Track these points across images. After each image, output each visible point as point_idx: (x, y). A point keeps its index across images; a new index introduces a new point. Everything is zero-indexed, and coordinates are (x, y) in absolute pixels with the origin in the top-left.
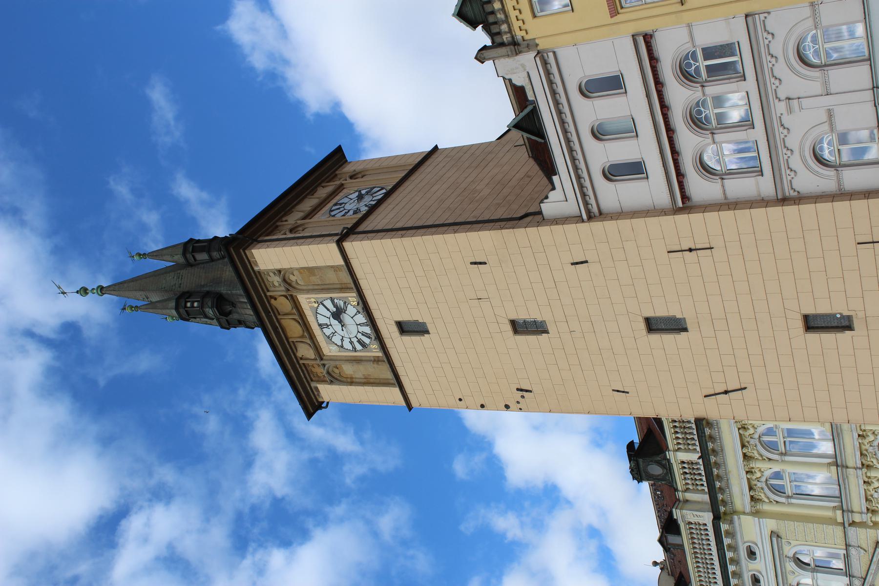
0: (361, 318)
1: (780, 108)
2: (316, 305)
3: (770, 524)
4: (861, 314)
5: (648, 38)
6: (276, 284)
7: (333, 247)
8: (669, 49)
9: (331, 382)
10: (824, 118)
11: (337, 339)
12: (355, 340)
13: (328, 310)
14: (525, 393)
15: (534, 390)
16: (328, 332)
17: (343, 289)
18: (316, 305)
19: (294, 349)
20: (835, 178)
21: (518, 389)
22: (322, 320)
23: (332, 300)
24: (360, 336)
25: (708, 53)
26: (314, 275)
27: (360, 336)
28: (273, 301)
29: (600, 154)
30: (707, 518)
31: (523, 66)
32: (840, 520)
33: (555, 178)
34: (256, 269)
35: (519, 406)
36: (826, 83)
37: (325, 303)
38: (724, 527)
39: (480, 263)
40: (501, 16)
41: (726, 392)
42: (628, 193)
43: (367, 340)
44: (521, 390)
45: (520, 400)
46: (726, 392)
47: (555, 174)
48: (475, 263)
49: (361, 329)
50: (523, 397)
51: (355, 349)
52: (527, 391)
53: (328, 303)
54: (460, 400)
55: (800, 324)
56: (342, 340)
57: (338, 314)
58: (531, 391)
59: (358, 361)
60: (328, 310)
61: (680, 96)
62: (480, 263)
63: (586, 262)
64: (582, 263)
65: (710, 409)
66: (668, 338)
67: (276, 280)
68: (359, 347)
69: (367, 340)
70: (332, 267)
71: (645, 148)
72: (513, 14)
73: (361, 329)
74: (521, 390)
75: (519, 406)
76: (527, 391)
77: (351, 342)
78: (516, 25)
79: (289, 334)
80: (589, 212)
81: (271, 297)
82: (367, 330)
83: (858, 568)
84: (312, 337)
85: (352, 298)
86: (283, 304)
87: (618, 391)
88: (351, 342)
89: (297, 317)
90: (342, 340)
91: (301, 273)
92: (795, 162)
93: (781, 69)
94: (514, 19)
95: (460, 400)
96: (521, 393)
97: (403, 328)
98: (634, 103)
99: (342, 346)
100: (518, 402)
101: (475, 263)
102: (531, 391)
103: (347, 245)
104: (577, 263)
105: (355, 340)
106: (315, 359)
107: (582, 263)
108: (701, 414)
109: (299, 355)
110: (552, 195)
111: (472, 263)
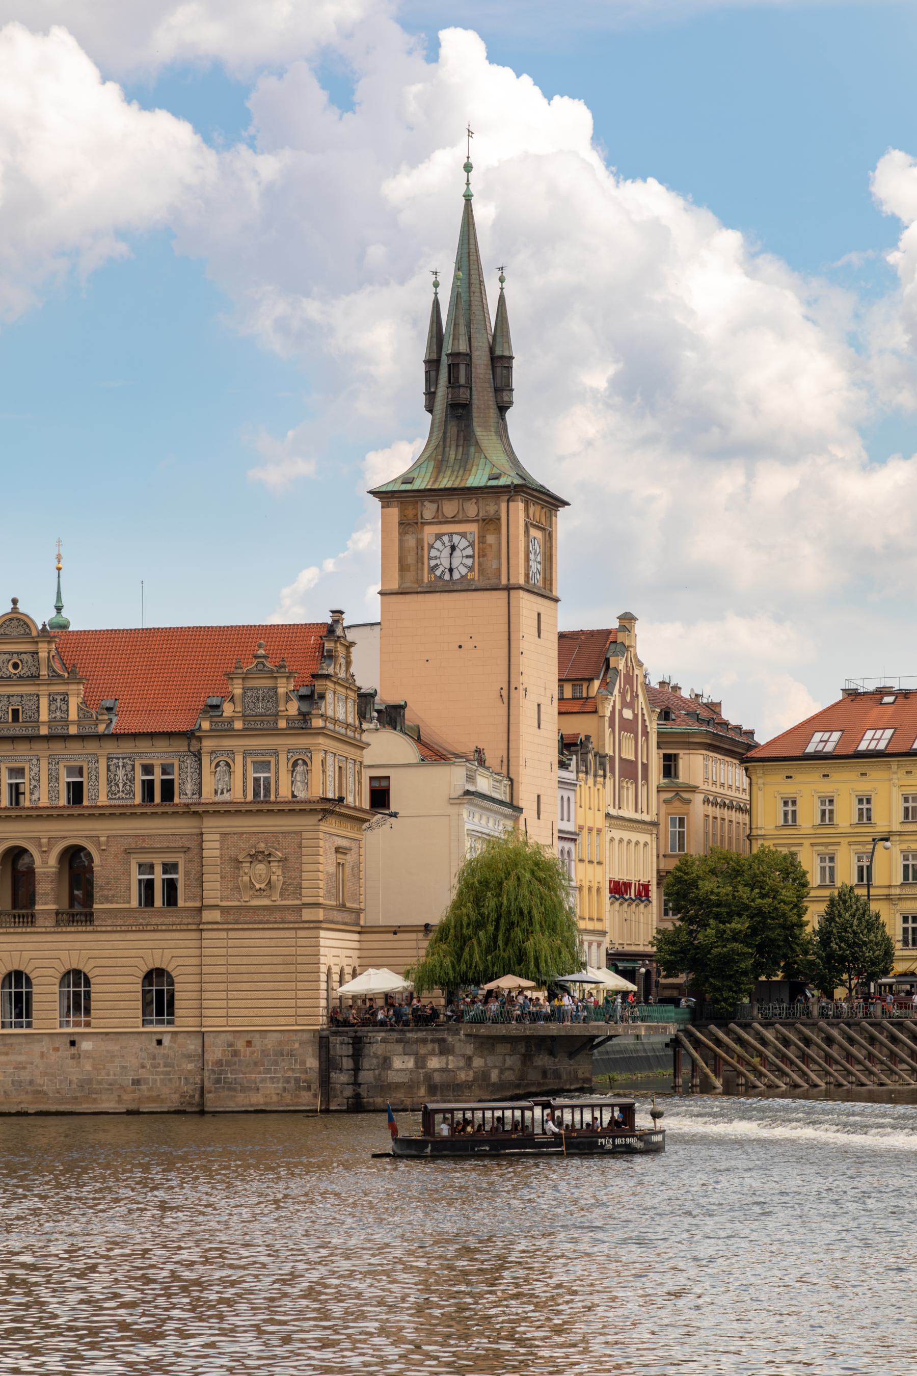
6: (488, 508)
11: (438, 544)
12: (438, 562)
16: (446, 539)
23: (472, 557)
28: (474, 500)
37: (470, 548)
43: (438, 573)
51: (430, 558)
53: (469, 551)
67: (492, 509)
68: (433, 563)
69: (438, 573)
77: (436, 558)
81: (478, 500)
84: (441, 523)
86: (471, 509)
88: (436, 558)
89: (460, 517)
105: (438, 562)
106: (422, 517)
109: (426, 503)
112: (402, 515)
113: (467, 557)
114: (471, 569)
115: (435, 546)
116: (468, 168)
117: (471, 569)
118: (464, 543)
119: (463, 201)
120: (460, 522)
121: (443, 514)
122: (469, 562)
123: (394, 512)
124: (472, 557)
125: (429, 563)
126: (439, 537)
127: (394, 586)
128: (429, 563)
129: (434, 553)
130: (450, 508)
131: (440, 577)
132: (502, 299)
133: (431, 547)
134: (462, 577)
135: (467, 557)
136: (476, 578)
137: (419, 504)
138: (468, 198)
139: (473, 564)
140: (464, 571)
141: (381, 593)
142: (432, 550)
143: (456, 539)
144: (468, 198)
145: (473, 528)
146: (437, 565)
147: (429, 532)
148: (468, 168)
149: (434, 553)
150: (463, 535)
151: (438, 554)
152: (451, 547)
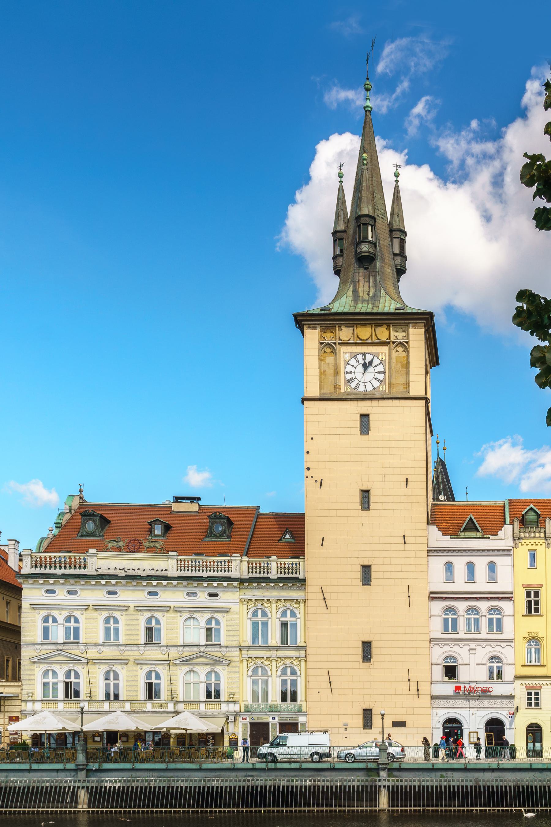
0: (369, 388)
1: (473, 645)
2: (380, 358)
3: (235, 608)
4: (371, 666)
5: (510, 598)
6: (397, 334)
7: (422, 393)
8: (505, 606)
9: (321, 344)
10: (465, 662)
11: (353, 362)
12: (353, 376)
13: (376, 366)
14: (319, 483)
15: (322, 491)
16: (360, 357)
18: (380, 358)
19: (347, 326)
20: (438, 663)
21: (322, 480)
23: (384, 372)
24: (356, 381)
25: (499, 621)
26: (402, 367)
27: (356, 381)
29: (460, 563)
30: (235, 574)
31: (508, 538)
32: (242, 644)
33: (448, 537)
34: (410, 325)
35: (309, 477)
36: (481, 664)
38: (235, 584)
39: (407, 484)
40: (532, 535)
41: (324, 599)
43: (353, 385)
44: (321, 482)
45: (314, 479)
46: (324, 599)
47: (451, 538)
48: (407, 481)
49: (362, 385)
50: (316, 481)
51: (346, 373)
52: (321, 486)
53: (380, 368)
54: (312, 439)
56: (353, 366)
57: (366, 366)
58: (320, 488)
59: (336, 373)
60: (376, 366)
61: (484, 606)
62: (407, 484)
63: (405, 543)
64: (405, 541)
65: (312, 588)
68: (348, 377)
70: (408, 383)
71: (460, 585)
72: (532, 541)
73: (362, 385)
74: (321, 482)
75: (309, 477)
76: (321, 486)
77: (351, 373)
78: (527, 541)
79: (359, 326)
80: (430, 550)
81: (389, 326)
82: (361, 389)
83: (209, 650)
84: (356, 344)
85: (385, 388)
86: (382, 333)
87: (323, 541)
88: (351, 373)
90: (353, 366)
91: (404, 357)
92: (447, 648)
93: (489, 648)
94: (530, 541)
95: (312, 439)
96: (319, 481)
97: (365, 418)
99: (348, 364)
100: (312, 477)
101: (407, 481)
102: (320, 488)
103: (423, 402)
104: (404, 538)
105: (353, 376)
107: (405, 541)
108: (308, 582)
110: (440, 533)
111: (407, 479)
113: (379, 372)
115: (350, 362)
120: (373, 344)
121: (358, 337)
122: (381, 377)
124: (384, 372)
125: (345, 377)
127: (316, 393)
128: (345, 377)
130: (365, 332)
131: (355, 389)
134: (374, 388)
135: (379, 372)
136: (387, 391)
137: (337, 326)
139: (384, 378)
142: (348, 366)
145: (385, 349)
146: (352, 379)
147: (345, 353)
149: (349, 369)
151: (353, 369)
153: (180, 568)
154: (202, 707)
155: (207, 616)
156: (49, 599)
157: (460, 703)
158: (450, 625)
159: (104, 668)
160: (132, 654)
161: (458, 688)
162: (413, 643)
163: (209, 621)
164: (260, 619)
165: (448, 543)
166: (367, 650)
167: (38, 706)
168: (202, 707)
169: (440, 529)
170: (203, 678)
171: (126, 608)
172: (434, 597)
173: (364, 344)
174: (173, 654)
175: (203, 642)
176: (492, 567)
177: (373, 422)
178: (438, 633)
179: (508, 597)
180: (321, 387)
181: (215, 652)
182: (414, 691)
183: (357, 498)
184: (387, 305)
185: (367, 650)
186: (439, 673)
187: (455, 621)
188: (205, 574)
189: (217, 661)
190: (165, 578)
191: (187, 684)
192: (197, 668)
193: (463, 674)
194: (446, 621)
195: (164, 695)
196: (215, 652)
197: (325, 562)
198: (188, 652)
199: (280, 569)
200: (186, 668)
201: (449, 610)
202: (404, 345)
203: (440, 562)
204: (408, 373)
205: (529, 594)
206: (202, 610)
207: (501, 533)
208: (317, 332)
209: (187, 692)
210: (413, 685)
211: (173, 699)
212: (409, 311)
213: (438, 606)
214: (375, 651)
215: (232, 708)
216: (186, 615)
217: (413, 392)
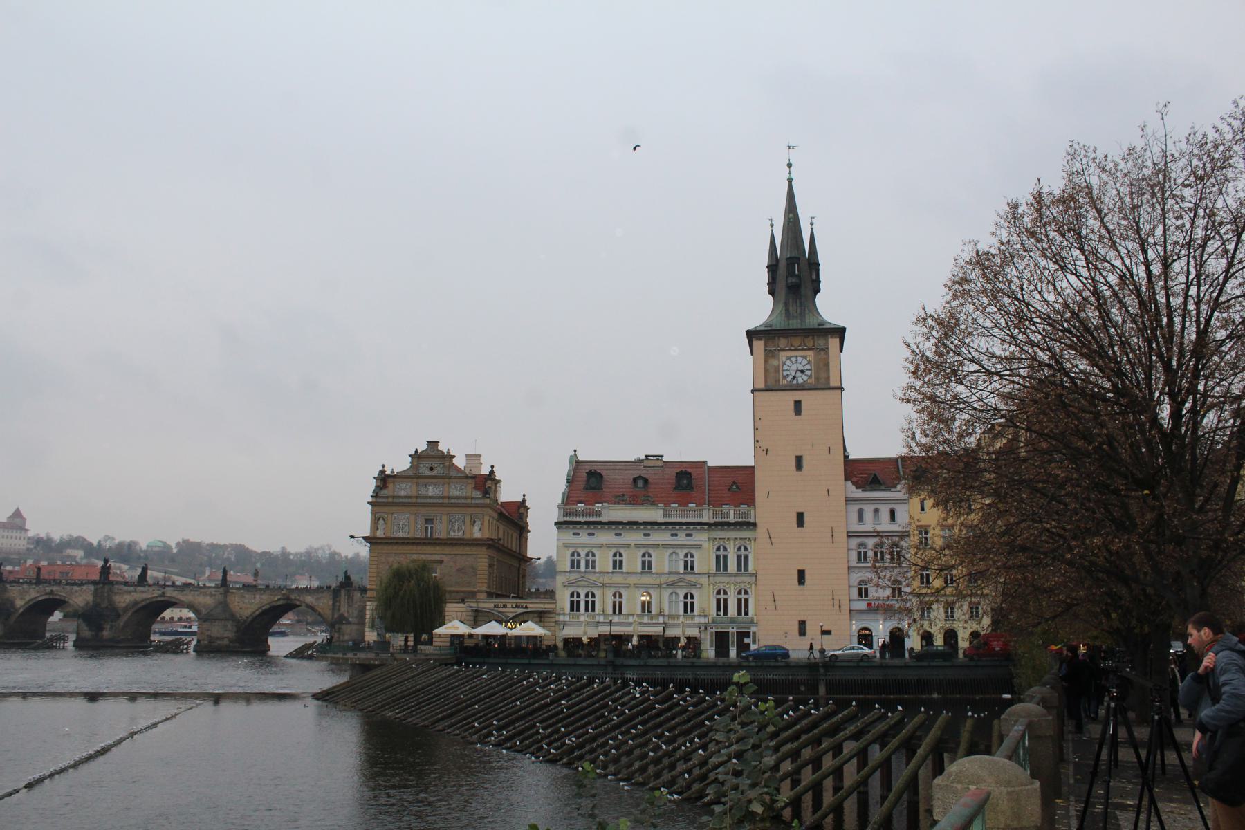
0: (800, 381)
3: (705, 545)
11: (788, 362)
17: (817, 379)
22: (800, 359)
30: (705, 520)
42: (855, 517)
53: (808, 367)
55: (801, 568)
59: (777, 370)
65: (761, 531)
66: (795, 520)
71: (868, 526)
85: (812, 381)
97: (798, 405)
98: (886, 526)
110: (853, 488)
112: (766, 346)
114: (810, 377)
116: (790, 165)
117: (810, 377)
118: (805, 362)
119: (787, 183)
123: (759, 345)
126: (789, 358)
127: (762, 386)
129: (785, 367)
130: (797, 342)
132: (812, 234)
133: (784, 364)
138: (790, 181)
140: (805, 378)
141: (753, 391)
143: (800, 359)
144: (790, 181)
147: (783, 356)
148: (790, 165)
149: (785, 367)
150: (805, 357)
152: (796, 363)
153: (665, 515)
154: (682, 619)
155: (685, 551)
156: (576, 540)
157: (871, 616)
158: (862, 557)
159: (613, 590)
160: (632, 580)
161: (869, 605)
162: (835, 570)
163: (686, 556)
164: (721, 553)
165: (860, 494)
166: (801, 575)
167: (567, 618)
168: (682, 619)
169: (854, 483)
170: (682, 598)
171: (628, 546)
172: (850, 535)
173: (796, 350)
174: (663, 580)
175: (682, 570)
176: (892, 513)
177: (804, 406)
178: (854, 563)
179: (904, 535)
180: (766, 382)
181: (691, 578)
182: (837, 607)
183: (793, 462)
184: (811, 322)
185: (801, 575)
186: (855, 592)
187: (865, 553)
188: (684, 520)
189: (693, 585)
190: (655, 523)
191: (670, 602)
192: (678, 591)
193: (872, 593)
194: (859, 553)
195: (654, 611)
196: (691, 578)
197: (770, 508)
198: (672, 578)
199: (737, 515)
200: (670, 591)
201: (861, 545)
202: (826, 350)
203: (855, 508)
204: (828, 370)
205: (920, 532)
206: (682, 547)
207: (899, 487)
208: (762, 343)
209: (670, 607)
210: (837, 603)
211: (660, 613)
212: (827, 326)
213: (854, 542)
214: (807, 577)
215: (703, 620)
216: (670, 551)
217: (832, 384)
